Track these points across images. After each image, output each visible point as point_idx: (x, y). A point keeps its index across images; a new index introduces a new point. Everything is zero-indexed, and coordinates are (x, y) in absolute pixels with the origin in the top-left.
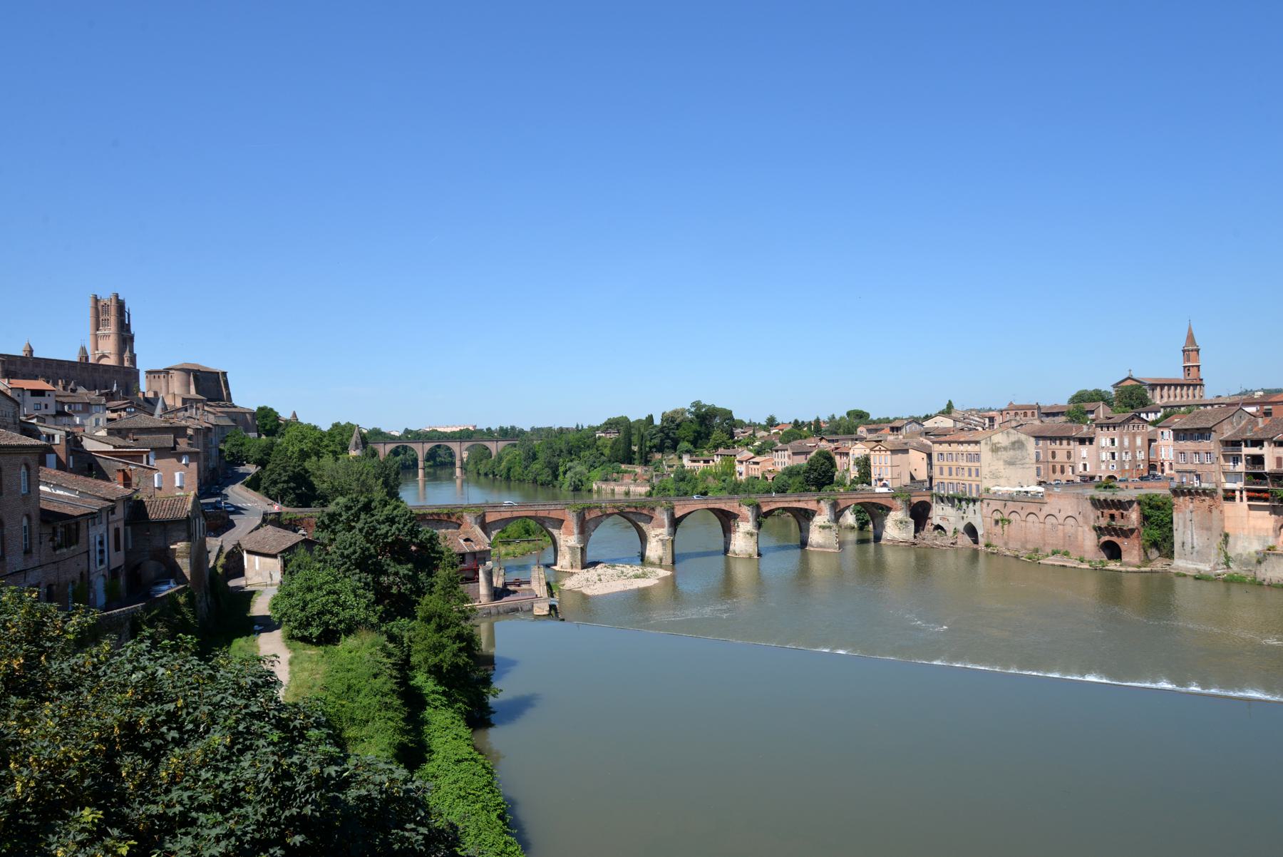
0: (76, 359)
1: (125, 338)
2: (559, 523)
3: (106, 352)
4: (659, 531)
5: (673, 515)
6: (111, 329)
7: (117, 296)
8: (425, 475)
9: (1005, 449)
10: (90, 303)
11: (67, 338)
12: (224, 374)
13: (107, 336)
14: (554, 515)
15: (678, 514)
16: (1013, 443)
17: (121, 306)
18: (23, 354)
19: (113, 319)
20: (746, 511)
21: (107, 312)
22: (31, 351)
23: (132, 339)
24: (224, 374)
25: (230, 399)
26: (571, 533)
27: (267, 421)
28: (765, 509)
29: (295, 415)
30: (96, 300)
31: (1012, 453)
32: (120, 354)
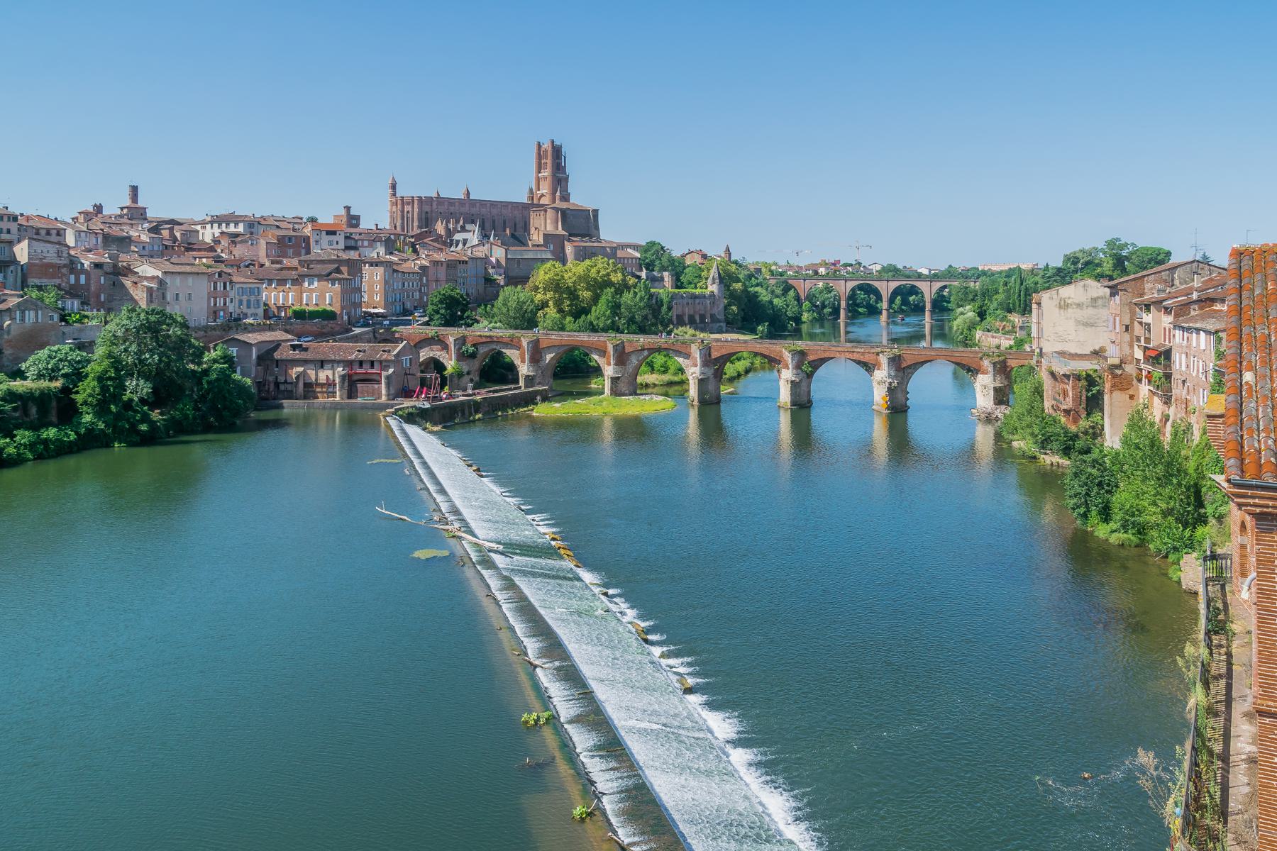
0: (525, 200)
1: (560, 181)
2: (603, 353)
3: (544, 192)
4: (693, 369)
6: (546, 173)
8: (847, 317)
9: (1079, 305)
10: (535, 150)
11: (513, 182)
12: (596, 212)
13: (545, 178)
15: (715, 354)
16: (1095, 300)
17: (557, 151)
19: (548, 161)
20: (788, 357)
22: (468, 194)
23: (567, 179)
24: (596, 212)
26: (609, 364)
27: (654, 258)
28: (811, 358)
29: (728, 249)
31: (1091, 311)
32: (554, 194)
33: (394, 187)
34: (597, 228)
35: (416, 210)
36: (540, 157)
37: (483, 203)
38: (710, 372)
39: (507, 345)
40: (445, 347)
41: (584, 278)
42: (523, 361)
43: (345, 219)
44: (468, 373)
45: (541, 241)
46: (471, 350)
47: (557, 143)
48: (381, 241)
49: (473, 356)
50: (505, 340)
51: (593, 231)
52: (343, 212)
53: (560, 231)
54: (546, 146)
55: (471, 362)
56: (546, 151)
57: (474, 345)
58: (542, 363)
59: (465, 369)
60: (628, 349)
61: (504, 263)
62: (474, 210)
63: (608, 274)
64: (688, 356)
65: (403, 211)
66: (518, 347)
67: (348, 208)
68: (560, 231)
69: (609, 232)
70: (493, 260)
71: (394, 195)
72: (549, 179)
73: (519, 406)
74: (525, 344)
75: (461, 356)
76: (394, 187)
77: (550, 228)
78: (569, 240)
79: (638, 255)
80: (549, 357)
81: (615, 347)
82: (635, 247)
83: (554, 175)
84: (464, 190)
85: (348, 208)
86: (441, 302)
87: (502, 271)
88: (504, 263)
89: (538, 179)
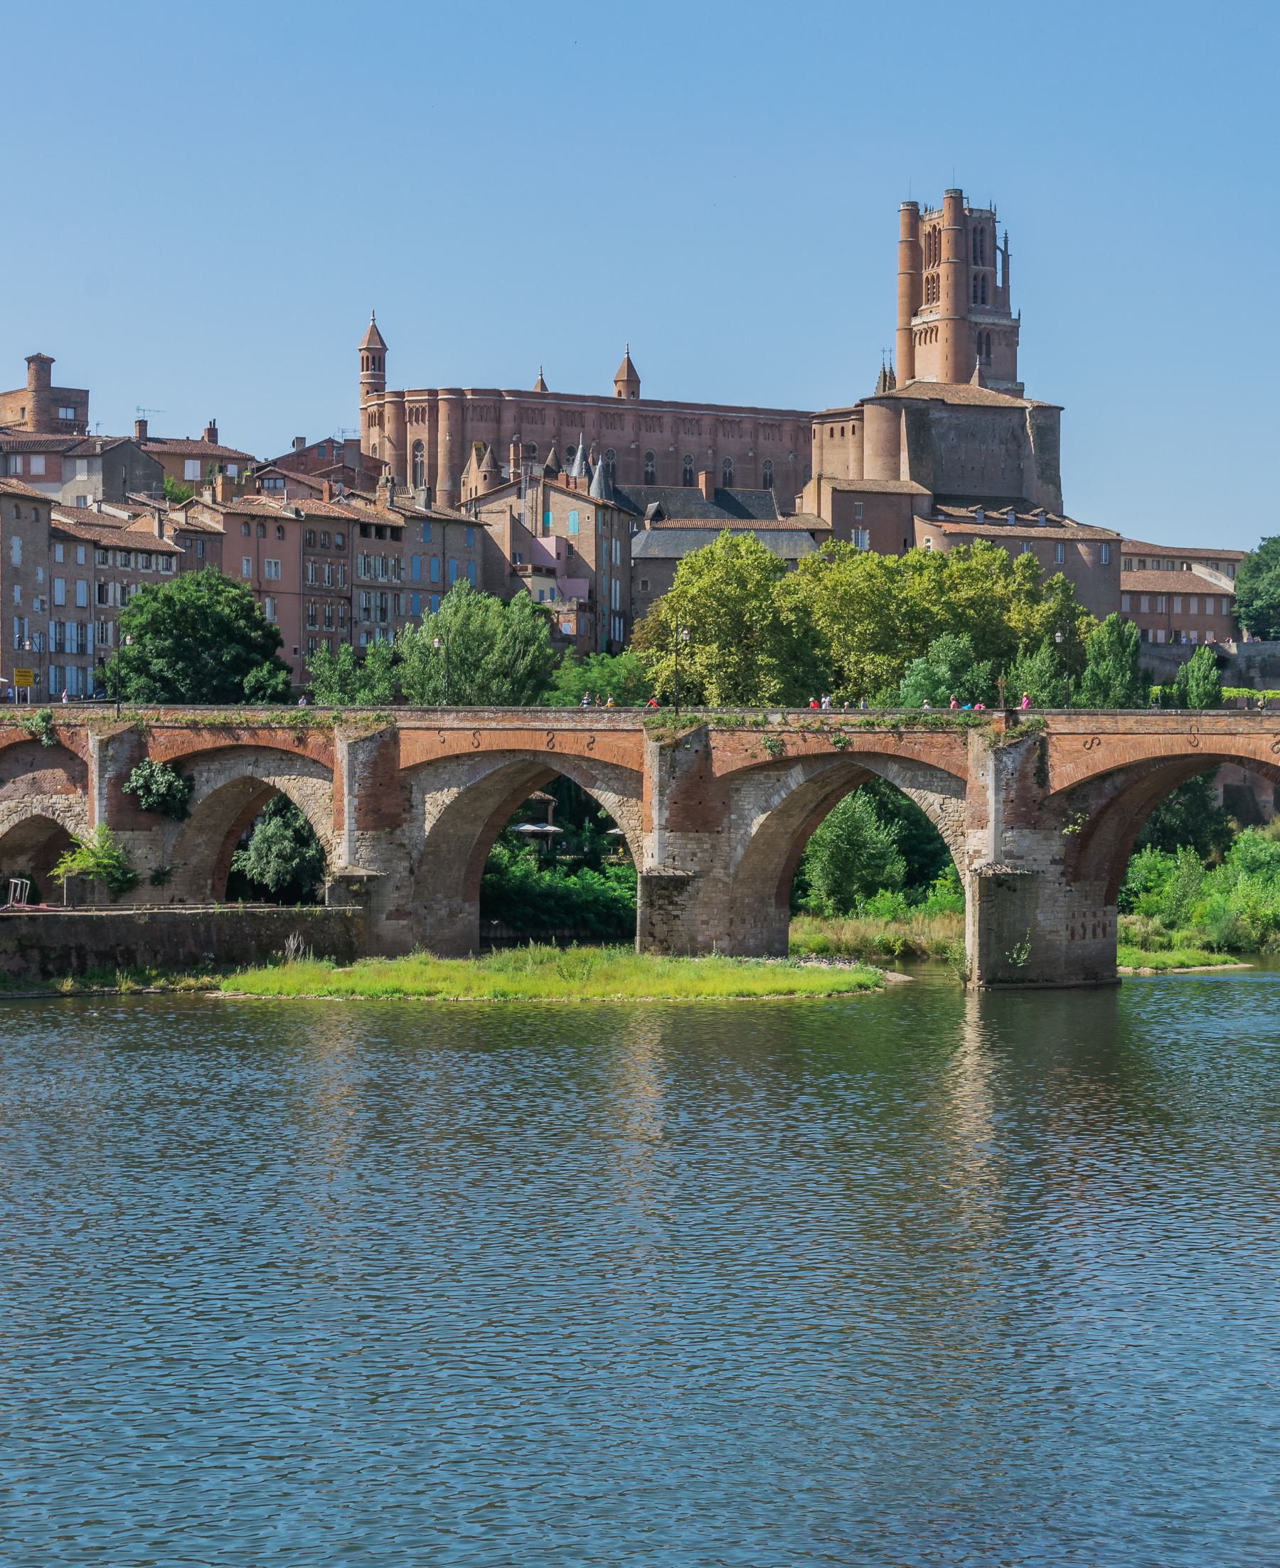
2: (629, 782)
5: (1042, 774)
6: (936, 313)
7: (957, 198)
11: (823, 343)
13: (931, 331)
14: (607, 749)
17: (976, 236)
18: (612, 391)
19: (943, 270)
21: (935, 258)
22: (632, 380)
23: (1012, 332)
24: (1049, 416)
25: (1057, 507)
30: (914, 214)
33: (375, 359)
34: (1051, 476)
35: (443, 437)
36: (918, 252)
37: (685, 415)
38: (1043, 851)
39: (288, 759)
40: (79, 778)
41: (849, 603)
42: (338, 826)
43: (29, 403)
44: (160, 878)
45: (827, 515)
46: (162, 781)
47: (975, 201)
48: (90, 456)
49: (172, 808)
50: (283, 739)
51: (1034, 487)
52: (22, 378)
53: (906, 481)
54: (939, 217)
55: (170, 833)
56: (935, 234)
57: (178, 765)
58: (407, 833)
59: (145, 859)
60: (728, 755)
61: (589, 557)
62: (657, 441)
63: (1004, 604)
64: (955, 785)
65: (399, 444)
66: (324, 770)
67: (41, 365)
68: (906, 481)
69: (1096, 496)
70: (549, 544)
71: (377, 386)
72: (944, 332)
73: (193, 965)
74: (341, 751)
75: (127, 810)
76: (375, 359)
77: (872, 474)
78: (933, 515)
79: (1226, 584)
80: (435, 803)
81: (670, 751)
82: (1214, 560)
83: (960, 319)
84: (616, 368)
85: (41, 365)
86: (154, 627)
87: (581, 587)
88: (589, 557)
89: (911, 337)
